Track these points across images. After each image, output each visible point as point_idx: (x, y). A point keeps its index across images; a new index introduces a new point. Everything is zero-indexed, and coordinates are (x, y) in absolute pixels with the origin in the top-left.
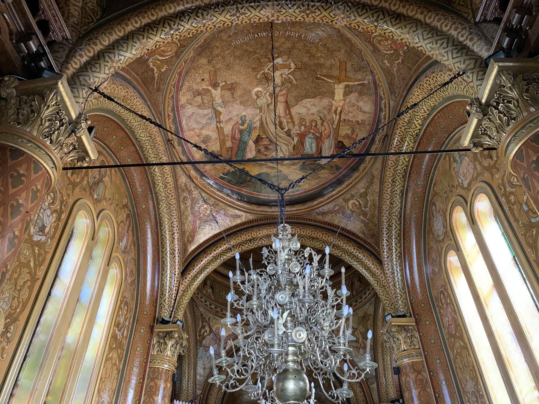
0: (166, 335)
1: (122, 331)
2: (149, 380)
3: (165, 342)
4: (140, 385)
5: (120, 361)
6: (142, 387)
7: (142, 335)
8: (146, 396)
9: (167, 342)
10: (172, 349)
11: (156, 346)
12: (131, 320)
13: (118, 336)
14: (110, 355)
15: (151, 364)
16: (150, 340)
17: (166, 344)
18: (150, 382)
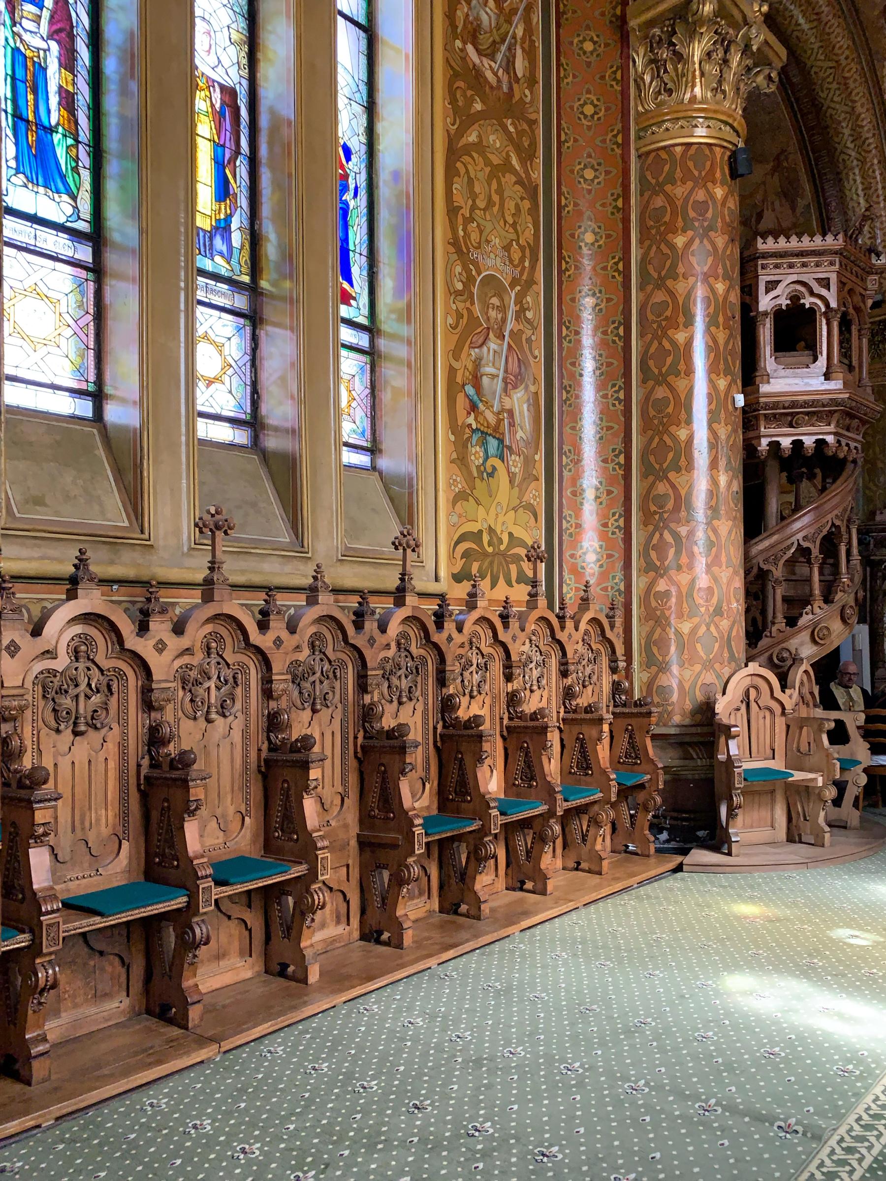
0: (673, 26)
1: (499, 57)
2: (647, 194)
3: (675, 52)
4: (619, 216)
5: (527, 156)
6: (626, 221)
7: (593, 59)
8: (647, 243)
9: (684, 52)
10: (707, 67)
11: (647, 78)
12: (537, 18)
13: (489, 75)
14: (473, 138)
15: (642, 142)
16: (625, 69)
17: (679, 57)
18: (650, 197)
